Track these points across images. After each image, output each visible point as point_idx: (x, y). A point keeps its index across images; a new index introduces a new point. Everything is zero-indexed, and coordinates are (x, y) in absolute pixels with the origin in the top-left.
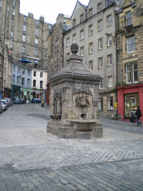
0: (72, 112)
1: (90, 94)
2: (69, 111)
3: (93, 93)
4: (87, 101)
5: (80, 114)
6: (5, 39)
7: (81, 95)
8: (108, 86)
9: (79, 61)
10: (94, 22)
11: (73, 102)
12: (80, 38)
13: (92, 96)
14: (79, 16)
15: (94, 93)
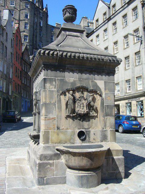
0: (58, 128)
1: (95, 91)
2: (52, 127)
3: (103, 90)
4: (90, 106)
5: (78, 131)
6: (34, 50)
7: (77, 95)
8: (137, 89)
9: (78, 34)
10: (119, 19)
11: (60, 108)
12: (104, 38)
13: (101, 96)
14: (102, 15)
15: (105, 90)
